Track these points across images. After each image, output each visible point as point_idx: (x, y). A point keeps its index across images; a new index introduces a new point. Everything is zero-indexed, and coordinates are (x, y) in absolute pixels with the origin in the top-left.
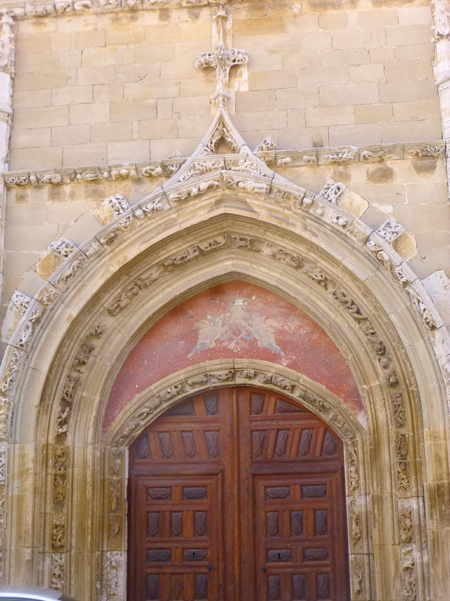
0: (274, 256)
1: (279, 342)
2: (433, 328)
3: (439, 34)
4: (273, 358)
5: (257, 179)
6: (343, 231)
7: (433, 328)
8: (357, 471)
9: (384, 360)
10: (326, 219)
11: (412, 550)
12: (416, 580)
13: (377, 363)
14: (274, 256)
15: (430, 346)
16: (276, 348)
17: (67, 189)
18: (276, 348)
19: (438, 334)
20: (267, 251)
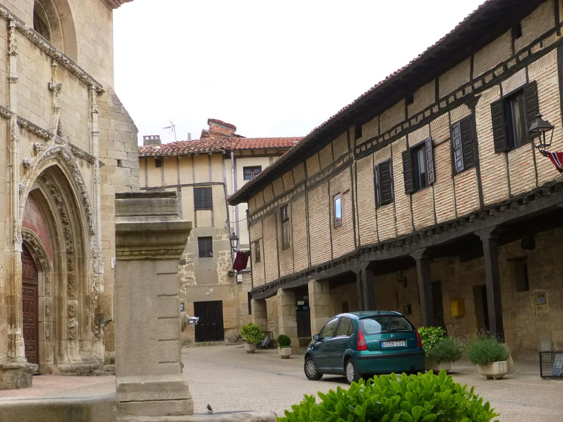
0: (48, 186)
1: (37, 224)
2: (93, 234)
3: (96, 110)
4: (36, 231)
5: (68, 154)
6: (78, 185)
7: (93, 234)
8: (49, 286)
9: (67, 242)
10: (76, 179)
11: (73, 321)
12: (76, 331)
13: (64, 242)
14: (48, 186)
15: (90, 241)
16: (36, 227)
17: (24, 130)
18: (36, 227)
19: (93, 237)
20: (48, 183)
